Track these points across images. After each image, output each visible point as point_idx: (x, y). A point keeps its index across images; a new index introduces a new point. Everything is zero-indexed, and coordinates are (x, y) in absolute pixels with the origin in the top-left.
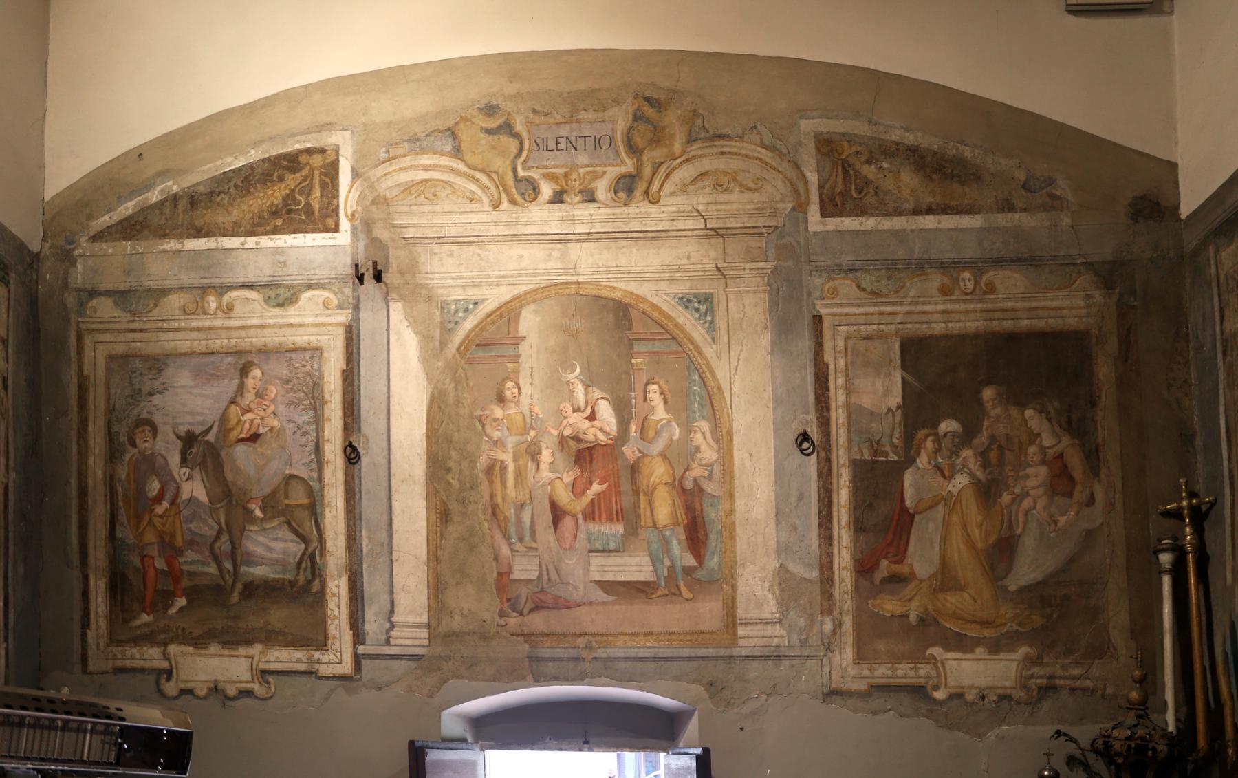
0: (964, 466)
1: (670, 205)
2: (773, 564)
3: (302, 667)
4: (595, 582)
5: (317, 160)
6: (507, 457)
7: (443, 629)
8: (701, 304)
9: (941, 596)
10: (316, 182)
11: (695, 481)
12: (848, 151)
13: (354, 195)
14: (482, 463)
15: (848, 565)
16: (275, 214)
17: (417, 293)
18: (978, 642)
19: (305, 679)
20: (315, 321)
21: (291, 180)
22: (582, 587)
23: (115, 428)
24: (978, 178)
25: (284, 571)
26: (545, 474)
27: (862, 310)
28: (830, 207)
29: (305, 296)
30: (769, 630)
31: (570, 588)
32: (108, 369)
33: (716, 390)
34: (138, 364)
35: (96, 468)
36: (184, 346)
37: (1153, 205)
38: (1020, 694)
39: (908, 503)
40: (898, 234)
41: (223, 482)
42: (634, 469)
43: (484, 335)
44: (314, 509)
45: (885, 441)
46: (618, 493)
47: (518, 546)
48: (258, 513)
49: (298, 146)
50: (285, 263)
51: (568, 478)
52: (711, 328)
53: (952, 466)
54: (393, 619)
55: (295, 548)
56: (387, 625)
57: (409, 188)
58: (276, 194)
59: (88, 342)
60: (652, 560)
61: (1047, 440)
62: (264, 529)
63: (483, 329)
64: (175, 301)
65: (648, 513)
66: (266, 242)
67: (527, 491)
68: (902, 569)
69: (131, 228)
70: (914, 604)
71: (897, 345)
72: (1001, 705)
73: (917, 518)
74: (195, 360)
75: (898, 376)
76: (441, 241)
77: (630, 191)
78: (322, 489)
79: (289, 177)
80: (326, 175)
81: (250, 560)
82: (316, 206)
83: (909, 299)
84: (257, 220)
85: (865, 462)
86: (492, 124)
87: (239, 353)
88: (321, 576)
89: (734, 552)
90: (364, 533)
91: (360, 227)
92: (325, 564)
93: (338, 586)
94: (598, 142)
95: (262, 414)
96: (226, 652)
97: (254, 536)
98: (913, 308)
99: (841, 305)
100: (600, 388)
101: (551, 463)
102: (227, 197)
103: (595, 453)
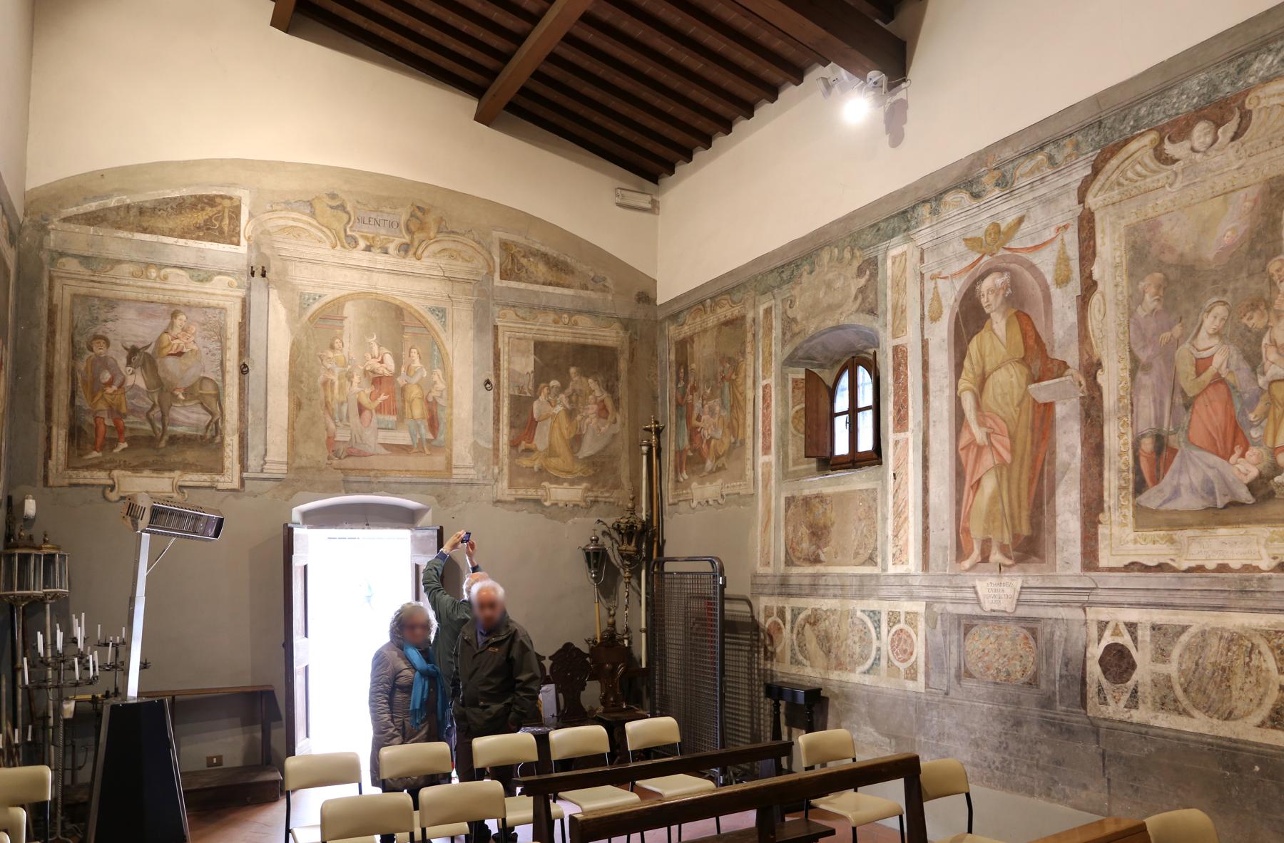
2: (471, 440)
3: (207, 484)
5: (227, 203)
7: (296, 465)
8: (440, 313)
10: (226, 215)
12: (514, 250)
13: (250, 228)
14: (321, 379)
16: (199, 228)
17: (285, 285)
18: (565, 480)
20: (223, 293)
23: (77, 338)
24: (573, 273)
26: (355, 388)
28: (505, 275)
29: (217, 278)
30: (468, 471)
32: (73, 302)
34: (96, 302)
35: (61, 361)
36: (132, 295)
37: (646, 298)
38: (583, 504)
39: (535, 416)
41: (158, 378)
42: (403, 390)
44: (218, 397)
48: (181, 397)
49: (214, 192)
51: (368, 391)
52: (444, 325)
55: (206, 418)
57: (283, 229)
58: (200, 218)
59: (57, 284)
61: (597, 393)
64: (126, 269)
66: (191, 243)
69: (93, 219)
72: (574, 509)
74: (139, 305)
75: (532, 357)
77: (406, 251)
79: (208, 209)
81: (174, 423)
82: (226, 229)
86: (334, 203)
87: (171, 304)
92: (224, 428)
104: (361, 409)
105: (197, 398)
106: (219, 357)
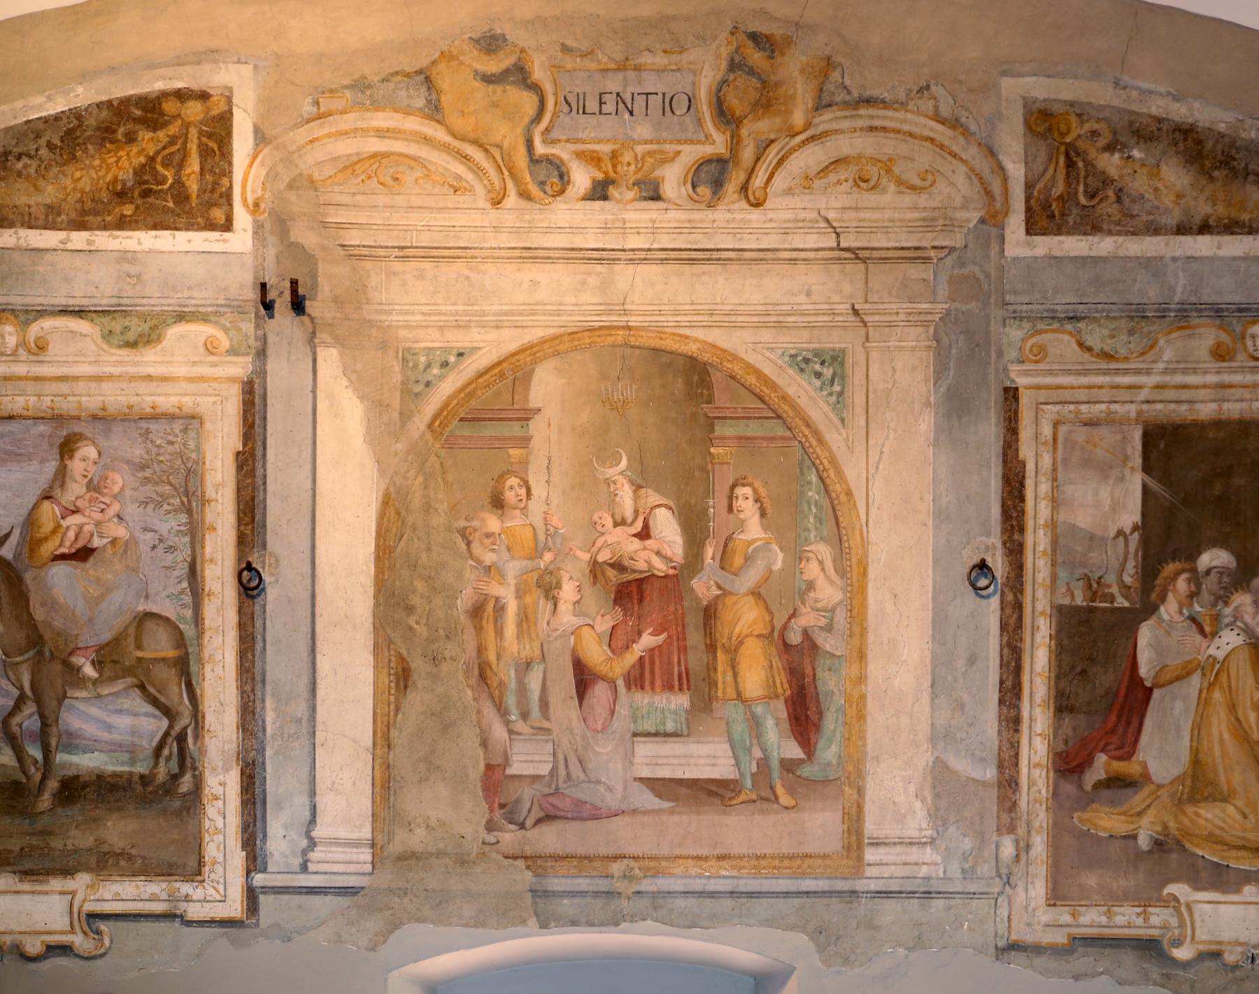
0: (1236, 618)
1: (781, 208)
2: (924, 759)
4: (641, 780)
5: (193, 110)
6: (507, 594)
7: (396, 847)
8: (827, 366)
9: (1190, 810)
10: (193, 146)
11: (806, 633)
12: (1077, 130)
13: (259, 172)
14: (465, 600)
15: (1044, 761)
16: (122, 195)
17: (361, 332)
19: (163, 926)
20: (192, 372)
21: (149, 141)
22: (620, 787)
25: (133, 762)
26: (567, 619)
27: (1084, 380)
28: (1043, 218)
30: (914, 854)
31: (601, 788)
33: (843, 498)
39: (1143, 671)
40: (1151, 264)
41: (30, 624)
42: (709, 614)
43: (473, 403)
44: (185, 667)
45: (1111, 578)
46: (683, 649)
47: (520, 726)
48: (89, 671)
49: (160, 86)
50: (139, 276)
51: (604, 625)
53: (1216, 618)
54: (314, 834)
55: (151, 725)
56: (304, 843)
57: (351, 166)
58: (123, 164)
60: (733, 748)
62: (99, 696)
63: (470, 395)
65: (729, 678)
67: (536, 645)
68: (1130, 768)
70: (1145, 821)
71: (1137, 435)
73: (1156, 693)
75: (1136, 481)
76: (404, 253)
77: (718, 185)
78: (200, 634)
79: (145, 135)
80: (210, 136)
81: (72, 742)
82: (193, 186)
83: (1161, 366)
84: (89, 205)
85: (1077, 609)
86: (493, 66)
87: (58, 419)
88: (195, 769)
89: (863, 738)
90: (269, 703)
91: (268, 226)
92: (202, 751)
93: (223, 784)
94: (669, 105)
95: (98, 516)
96: (26, 887)
97: (81, 706)
98: (1167, 379)
99: (1050, 372)
100: (658, 490)
101: (578, 602)
102: (34, 164)
103: (648, 588)
104: (584, 679)
105: (129, 672)
106: (184, 554)
